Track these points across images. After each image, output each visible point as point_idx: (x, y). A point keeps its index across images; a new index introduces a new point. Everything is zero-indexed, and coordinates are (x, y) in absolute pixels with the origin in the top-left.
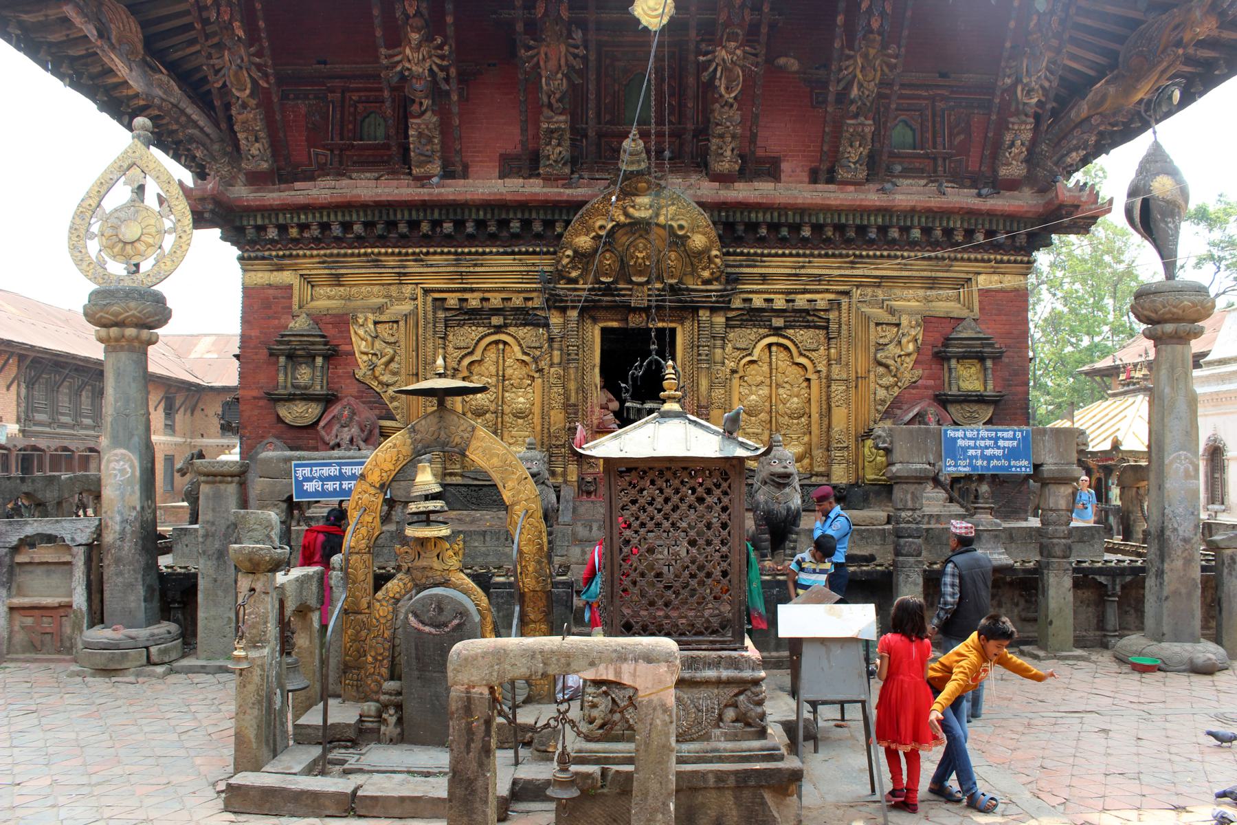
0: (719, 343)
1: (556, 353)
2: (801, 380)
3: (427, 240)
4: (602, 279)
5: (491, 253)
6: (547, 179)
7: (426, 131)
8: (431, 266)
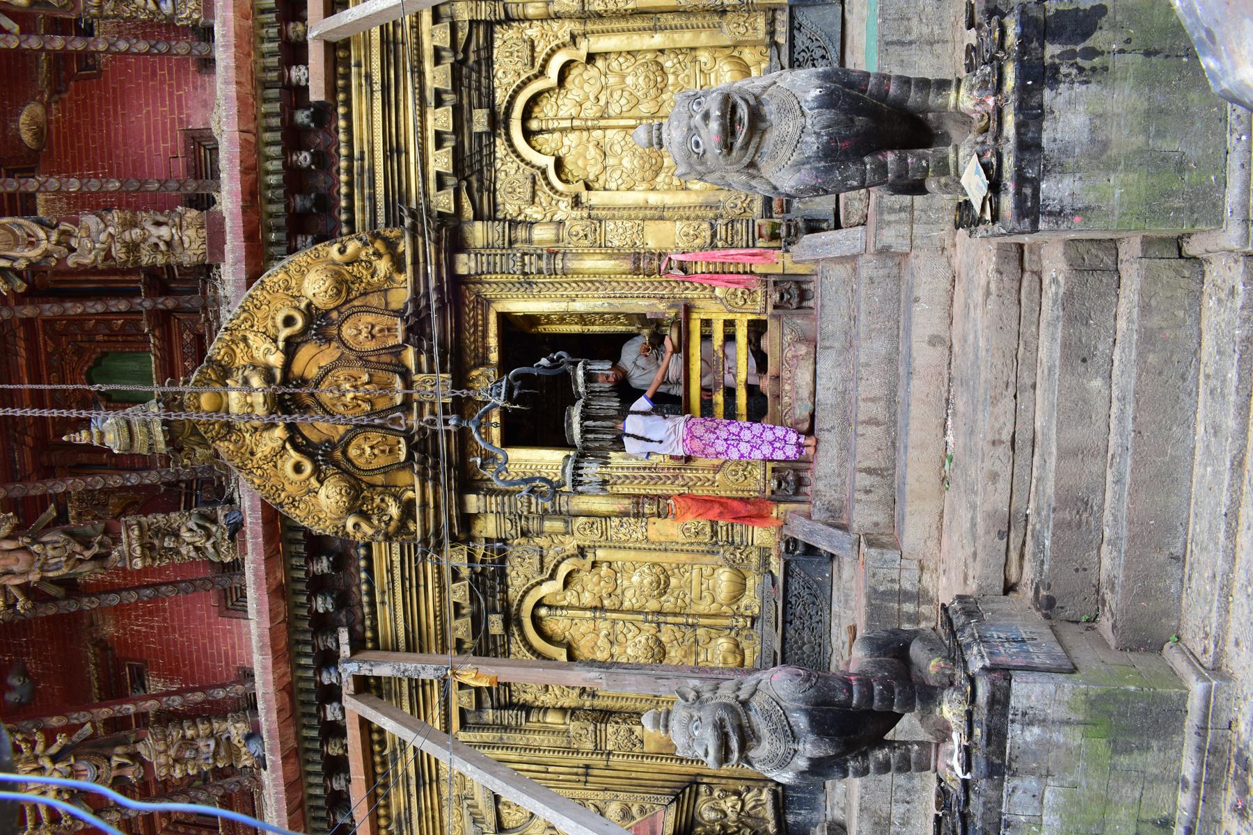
0: (521, 233)
1: (548, 525)
2: (592, 72)
4: (403, 457)
7: (172, 752)
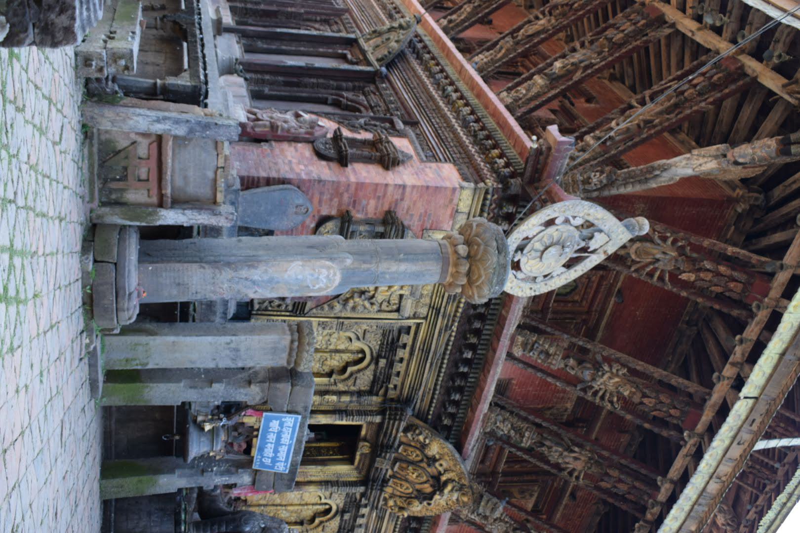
3: (462, 335)
5: (438, 376)
6: (486, 419)
8: (439, 335)
